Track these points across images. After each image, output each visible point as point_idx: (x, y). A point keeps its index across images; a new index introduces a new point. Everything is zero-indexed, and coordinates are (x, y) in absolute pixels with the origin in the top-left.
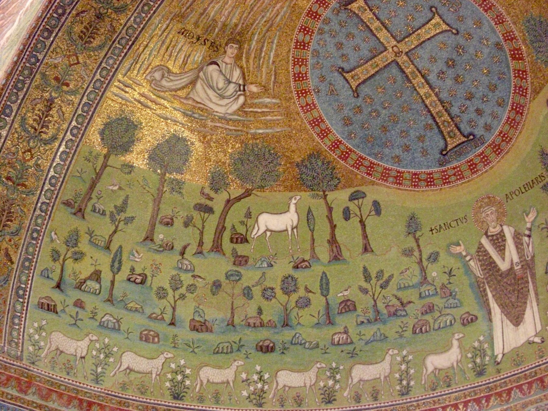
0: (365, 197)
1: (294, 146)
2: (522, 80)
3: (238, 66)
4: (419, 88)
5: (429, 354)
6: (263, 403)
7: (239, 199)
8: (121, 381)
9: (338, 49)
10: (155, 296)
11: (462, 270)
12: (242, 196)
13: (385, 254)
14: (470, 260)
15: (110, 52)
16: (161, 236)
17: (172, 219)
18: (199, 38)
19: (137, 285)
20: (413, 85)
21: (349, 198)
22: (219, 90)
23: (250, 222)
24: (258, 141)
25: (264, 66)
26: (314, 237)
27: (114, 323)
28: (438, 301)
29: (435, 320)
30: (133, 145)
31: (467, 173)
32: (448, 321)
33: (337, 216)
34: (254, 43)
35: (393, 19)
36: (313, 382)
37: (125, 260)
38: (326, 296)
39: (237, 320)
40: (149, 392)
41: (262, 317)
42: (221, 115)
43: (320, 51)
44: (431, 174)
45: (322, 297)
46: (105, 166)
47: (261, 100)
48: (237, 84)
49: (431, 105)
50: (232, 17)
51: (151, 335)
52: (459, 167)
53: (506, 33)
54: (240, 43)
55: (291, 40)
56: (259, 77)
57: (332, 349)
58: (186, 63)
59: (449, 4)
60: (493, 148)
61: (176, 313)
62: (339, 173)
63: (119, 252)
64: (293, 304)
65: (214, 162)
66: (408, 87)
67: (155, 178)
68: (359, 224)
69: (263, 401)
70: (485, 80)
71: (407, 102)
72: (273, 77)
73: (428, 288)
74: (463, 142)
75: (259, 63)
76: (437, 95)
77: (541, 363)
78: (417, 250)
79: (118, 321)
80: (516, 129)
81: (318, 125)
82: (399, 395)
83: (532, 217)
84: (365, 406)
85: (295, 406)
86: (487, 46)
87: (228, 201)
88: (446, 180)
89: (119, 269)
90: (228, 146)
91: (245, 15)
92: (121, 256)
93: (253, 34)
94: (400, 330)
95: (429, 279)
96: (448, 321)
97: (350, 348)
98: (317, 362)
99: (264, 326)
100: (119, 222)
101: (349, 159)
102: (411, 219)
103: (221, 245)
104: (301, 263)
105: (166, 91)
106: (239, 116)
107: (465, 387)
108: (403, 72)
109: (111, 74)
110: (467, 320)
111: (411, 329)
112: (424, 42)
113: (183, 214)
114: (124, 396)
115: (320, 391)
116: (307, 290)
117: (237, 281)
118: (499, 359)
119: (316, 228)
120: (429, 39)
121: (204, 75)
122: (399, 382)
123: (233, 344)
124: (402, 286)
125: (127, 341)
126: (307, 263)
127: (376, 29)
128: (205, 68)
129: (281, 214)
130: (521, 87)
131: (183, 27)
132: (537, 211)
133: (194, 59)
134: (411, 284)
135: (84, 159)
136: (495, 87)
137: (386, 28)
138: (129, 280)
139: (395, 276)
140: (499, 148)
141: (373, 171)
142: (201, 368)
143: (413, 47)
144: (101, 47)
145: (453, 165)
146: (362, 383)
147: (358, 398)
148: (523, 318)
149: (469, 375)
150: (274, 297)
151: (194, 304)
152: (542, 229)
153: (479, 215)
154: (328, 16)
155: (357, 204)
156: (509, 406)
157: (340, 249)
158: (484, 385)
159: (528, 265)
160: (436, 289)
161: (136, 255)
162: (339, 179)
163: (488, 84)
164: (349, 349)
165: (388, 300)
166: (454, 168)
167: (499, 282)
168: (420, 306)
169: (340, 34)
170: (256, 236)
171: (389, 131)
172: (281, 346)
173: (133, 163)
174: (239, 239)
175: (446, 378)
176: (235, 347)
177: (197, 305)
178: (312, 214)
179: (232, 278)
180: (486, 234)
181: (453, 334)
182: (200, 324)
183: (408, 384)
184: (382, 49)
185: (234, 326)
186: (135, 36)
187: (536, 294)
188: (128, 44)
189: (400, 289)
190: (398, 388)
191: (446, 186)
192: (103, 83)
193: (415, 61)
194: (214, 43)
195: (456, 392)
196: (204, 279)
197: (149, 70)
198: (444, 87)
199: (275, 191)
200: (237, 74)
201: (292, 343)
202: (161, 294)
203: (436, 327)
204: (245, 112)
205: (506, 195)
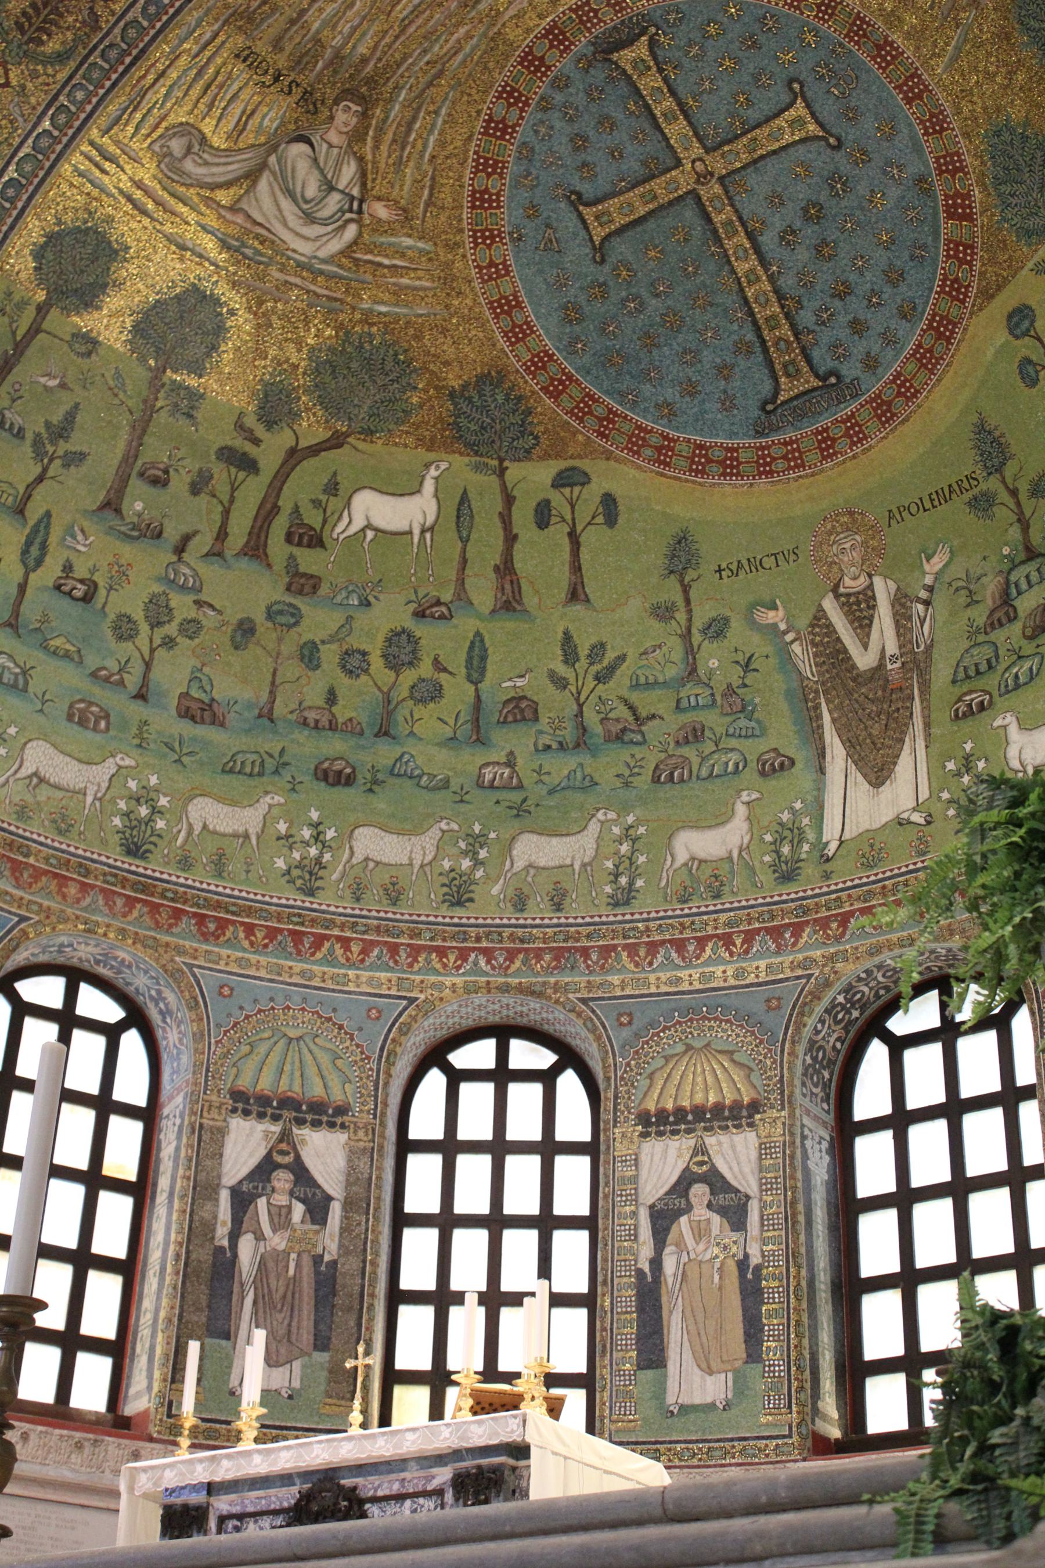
0: (589, 483)
1: (450, 352)
2: (960, 267)
3: (355, 153)
5: (683, 827)
6: (318, 888)
7: (315, 450)
8: (16, 799)
9: (577, 149)
10: (109, 633)
11: (773, 661)
12: (324, 446)
13: (613, 610)
14: (792, 642)
15: (81, 72)
16: (139, 506)
17: (166, 472)
18: (280, 75)
19: (74, 603)
20: (725, 251)
21: (554, 481)
22: (307, 202)
23: (334, 504)
24: (374, 329)
25: (411, 164)
26: (468, 556)
27: (16, 675)
28: (714, 720)
29: (703, 759)
30: (104, 293)
31: (813, 457)
32: (731, 764)
33: (523, 516)
34: (397, 107)
35: (705, 97)
36: (429, 858)
37: (54, 544)
38: (476, 684)
39: (279, 709)
40: (75, 831)
41: (334, 709)
42: (303, 259)
43: (537, 148)
44: (736, 450)
46: (35, 330)
47: (393, 239)
48: (347, 194)
49: (756, 301)
50: (359, 40)
51: (92, 713)
52: (797, 441)
53: (944, 157)
54: (366, 103)
55: (479, 112)
56: (397, 187)
58: (244, 129)
59: (830, 78)
60: (875, 409)
61: (152, 676)
62: (540, 423)
63: (43, 525)
64: (405, 693)
65: (272, 361)
66: (713, 255)
67: (138, 375)
68: (567, 540)
69: (319, 883)
70: (881, 258)
72: (426, 192)
74: (814, 389)
75: (401, 157)
76: (771, 279)
78: (683, 609)
79: (24, 673)
81: (509, 313)
82: (609, 904)
83: (937, 563)
84: (534, 919)
85: (385, 902)
86: (898, 182)
87: (292, 452)
88: (765, 468)
89: (39, 562)
90: (309, 330)
91: (387, 40)
92: (48, 534)
93: (397, 88)
94: (627, 773)
95: (701, 672)
96: (731, 764)
97: (516, 797)
99: (336, 730)
100: (51, 460)
101: (564, 397)
102: (679, 542)
104: (432, 606)
105: (192, 185)
106: (340, 266)
107: (752, 902)
108: (709, 220)
109: (77, 124)
110: (772, 764)
111: (650, 773)
112: (762, 157)
113: (192, 465)
114: (20, 832)
116: (439, 666)
119: (474, 536)
120: (774, 152)
121: (279, 162)
122: (612, 878)
123: (265, 756)
124: (642, 680)
125: (41, 719)
126: (444, 609)
127: (664, 115)
128: (283, 146)
129: (401, 495)
130: (956, 280)
131: (248, 44)
132: (951, 552)
133: (261, 124)
134: (661, 679)
136: (901, 275)
137: (687, 117)
138: (58, 587)
142: (191, 799)
143: (738, 165)
144: (61, 58)
145: (787, 437)
146: (532, 871)
147: (520, 903)
148: (892, 771)
150: (366, 671)
152: (957, 590)
153: (825, 547)
154: (566, 71)
155: (568, 496)
156: (841, 948)
157: (520, 588)
158: (793, 900)
159: (915, 661)
160: (712, 695)
161: (80, 537)
162: (536, 438)
163: (886, 268)
164: (514, 799)
165: (608, 708)
166: (786, 444)
167: (850, 693)
168: (676, 727)
169: (586, 117)
170: (342, 537)
171: (658, 346)
172: (369, 776)
173: (99, 334)
174: (305, 540)
177: (199, 666)
178: (469, 506)
182: (201, 705)
183: (631, 883)
184: (670, 162)
185: (272, 721)
186: (141, 45)
187: (927, 725)
188: (123, 63)
189: (636, 686)
190: (608, 889)
192: (57, 140)
193: (737, 198)
194: (311, 94)
195: (730, 910)
196: (220, 612)
197: (160, 131)
198: (791, 264)
199: (396, 444)
200: (349, 171)
201: (392, 773)
202: (124, 628)
203: (704, 773)
204: (356, 261)
205: (890, 511)
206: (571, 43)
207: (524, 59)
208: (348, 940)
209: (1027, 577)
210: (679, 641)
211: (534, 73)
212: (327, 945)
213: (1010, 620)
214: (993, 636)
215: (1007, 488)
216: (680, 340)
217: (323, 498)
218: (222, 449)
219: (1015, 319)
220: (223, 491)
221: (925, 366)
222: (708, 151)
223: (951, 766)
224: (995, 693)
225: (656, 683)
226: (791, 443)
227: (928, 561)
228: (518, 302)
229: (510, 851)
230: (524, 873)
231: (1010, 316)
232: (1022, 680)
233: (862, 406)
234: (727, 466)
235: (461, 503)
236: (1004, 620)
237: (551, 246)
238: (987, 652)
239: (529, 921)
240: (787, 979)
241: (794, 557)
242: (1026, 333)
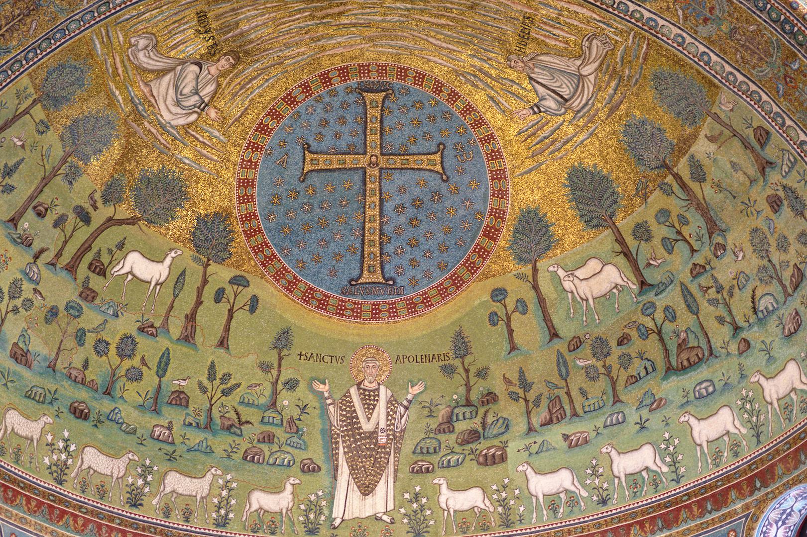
3: (218, 82)
6: (64, 480)
7: (121, 222)
11: (317, 412)
14: (330, 404)
16: (26, 225)
17: (46, 210)
21: (231, 279)
22: (181, 94)
28: (280, 434)
31: (367, 315)
35: (396, 131)
36: (121, 474)
39: (59, 366)
42: (163, 121)
44: (329, 297)
45: (156, 377)
53: (496, 209)
54: (238, 59)
57: (149, 442)
64: (123, 373)
68: (227, 312)
71: (347, 214)
73: (274, 415)
75: (238, 92)
76: (381, 224)
80: (443, 298)
82: (214, 524)
83: (416, 390)
85: (97, 496)
87: (110, 219)
88: (340, 312)
94: (230, 450)
96: (286, 460)
97: (170, 449)
98: (130, 452)
102: (284, 333)
103: (77, 267)
104: (149, 327)
108: (365, 184)
113: (60, 210)
115: (127, 488)
116: (143, 362)
117: (76, 317)
120: (413, 169)
123: (47, 392)
124: (246, 401)
126: (154, 330)
127: (371, 129)
129: (153, 261)
134: (256, 403)
135: (15, 92)
139: (241, 387)
140: (414, 308)
146: (175, 495)
147: (167, 513)
149: (298, 529)
151: (24, 325)
152: (424, 407)
154: (338, 89)
165: (226, 411)
166: (355, 303)
170: (116, 274)
171: (310, 232)
172: (96, 417)
174: (98, 270)
175: (271, 523)
176: (49, 397)
177: (26, 328)
179: (72, 312)
180: (359, 385)
182: (21, 352)
183: (227, 514)
185: (54, 371)
187: (396, 471)
189: (242, 403)
196: (44, 299)
200: (210, 88)
203: (271, 461)
204: (187, 132)
206: (349, 79)
207: (322, 75)
208: (77, 516)
209: (464, 413)
210: (270, 385)
211: (323, 83)
212: (66, 517)
213: (450, 432)
214: (439, 436)
217: (114, 249)
218: (77, 206)
220: (69, 229)
222: (382, 154)
223: (407, 496)
224: (436, 466)
225: (253, 404)
227: (412, 387)
228: (253, 184)
229: (164, 480)
230: (170, 495)
231: (494, 291)
232: (452, 464)
234: (321, 304)
235: (181, 275)
236: (446, 430)
237: (283, 164)
238: (435, 444)
239: (171, 525)
241: (341, 361)
242: (499, 301)
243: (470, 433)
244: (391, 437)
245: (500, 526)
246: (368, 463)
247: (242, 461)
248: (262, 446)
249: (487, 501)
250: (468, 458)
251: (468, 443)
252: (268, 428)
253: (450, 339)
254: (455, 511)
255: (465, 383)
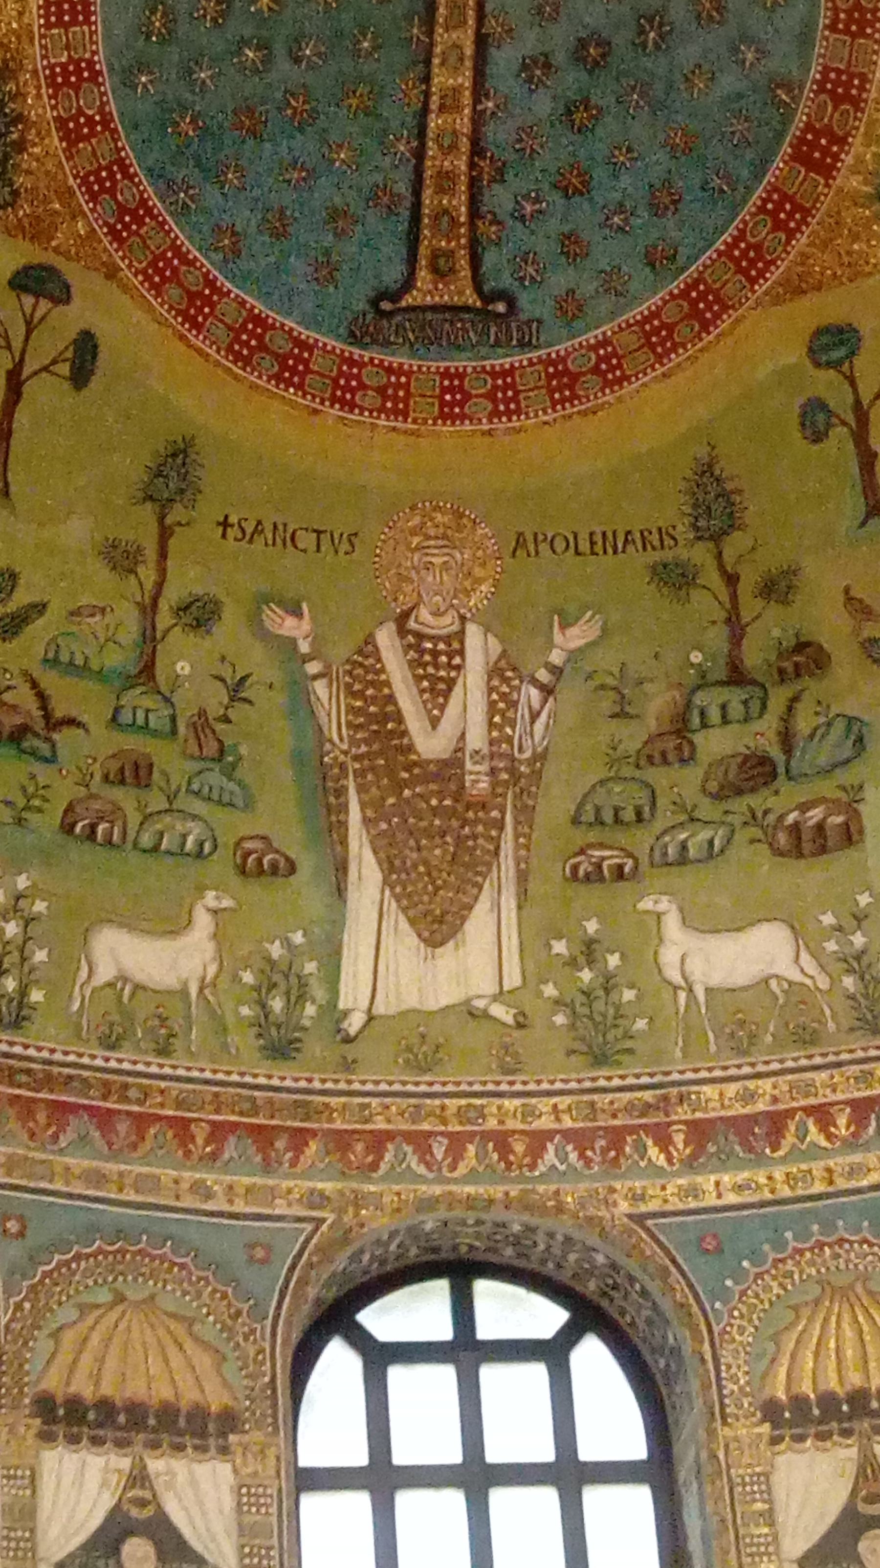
4: (443, 64)
11: (280, 698)
14: (315, 677)
20: (432, 45)
44: (310, 349)
49: (438, 139)
52: (409, 374)
53: (839, 72)
60: (550, 377)
62: (29, 172)
73: (151, 705)
74: (466, 309)
76: (478, 119)
77: (504, 1087)
80: (659, 358)
94: (21, 802)
96: (190, 840)
102: (174, 455)
110: (260, 861)
111: (60, 813)
118: (355, 1023)
124: (64, 657)
134: (95, 665)
141: (137, 233)
145: (396, 361)
152: (603, 687)
158: (288, 1090)
160: (173, 719)
166: (390, 370)
175: (157, 1022)
180: (402, 619)
181: (200, 890)
183: (23, 991)
187: (522, 877)
189: (51, 662)
191: (336, 411)
195: (190, 1080)
203: (146, 840)
205: (520, 535)
210: (135, 613)
215: (721, 567)
216: (294, 143)
219: (825, 339)
221: (652, 347)
223: (560, 947)
224: (644, 860)
225: (86, 666)
226: (399, 371)
227: (563, 627)
231: (819, 332)
232: (692, 852)
233: (531, 363)
236: (671, 757)
240: (280, 1218)
243: (744, 762)
244: (505, 776)
245: (852, 1029)
246: (437, 852)
247: (60, 838)
248: (118, 794)
249: (805, 958)
250: (742, 836)
251: (740, 792)
252: (131, 742)
253: (682, 485)
254: (708, 990)
255: (724, 615)
